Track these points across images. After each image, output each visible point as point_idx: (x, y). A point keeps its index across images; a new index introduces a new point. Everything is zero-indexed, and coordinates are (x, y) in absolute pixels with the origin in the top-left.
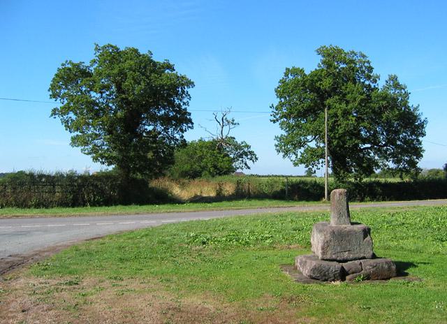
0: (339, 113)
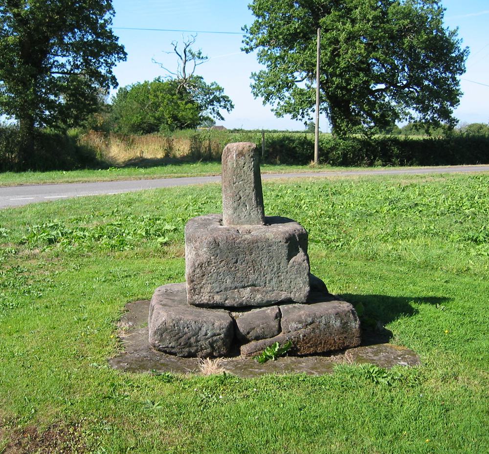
0: (343, 37)
